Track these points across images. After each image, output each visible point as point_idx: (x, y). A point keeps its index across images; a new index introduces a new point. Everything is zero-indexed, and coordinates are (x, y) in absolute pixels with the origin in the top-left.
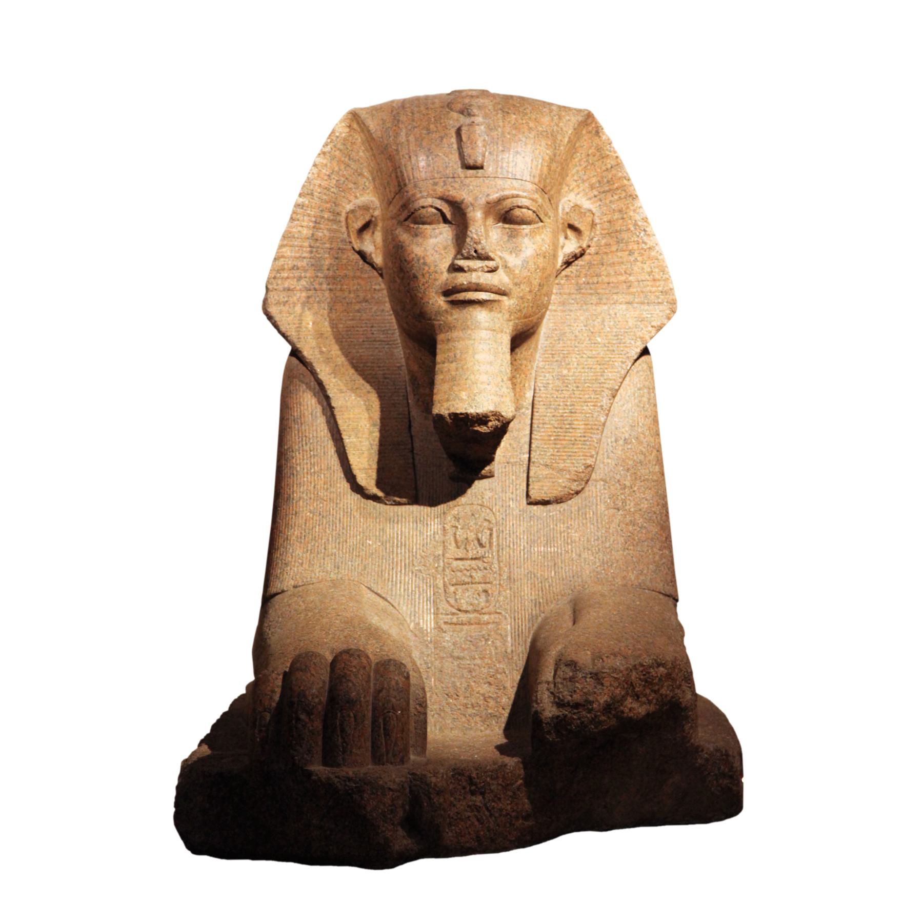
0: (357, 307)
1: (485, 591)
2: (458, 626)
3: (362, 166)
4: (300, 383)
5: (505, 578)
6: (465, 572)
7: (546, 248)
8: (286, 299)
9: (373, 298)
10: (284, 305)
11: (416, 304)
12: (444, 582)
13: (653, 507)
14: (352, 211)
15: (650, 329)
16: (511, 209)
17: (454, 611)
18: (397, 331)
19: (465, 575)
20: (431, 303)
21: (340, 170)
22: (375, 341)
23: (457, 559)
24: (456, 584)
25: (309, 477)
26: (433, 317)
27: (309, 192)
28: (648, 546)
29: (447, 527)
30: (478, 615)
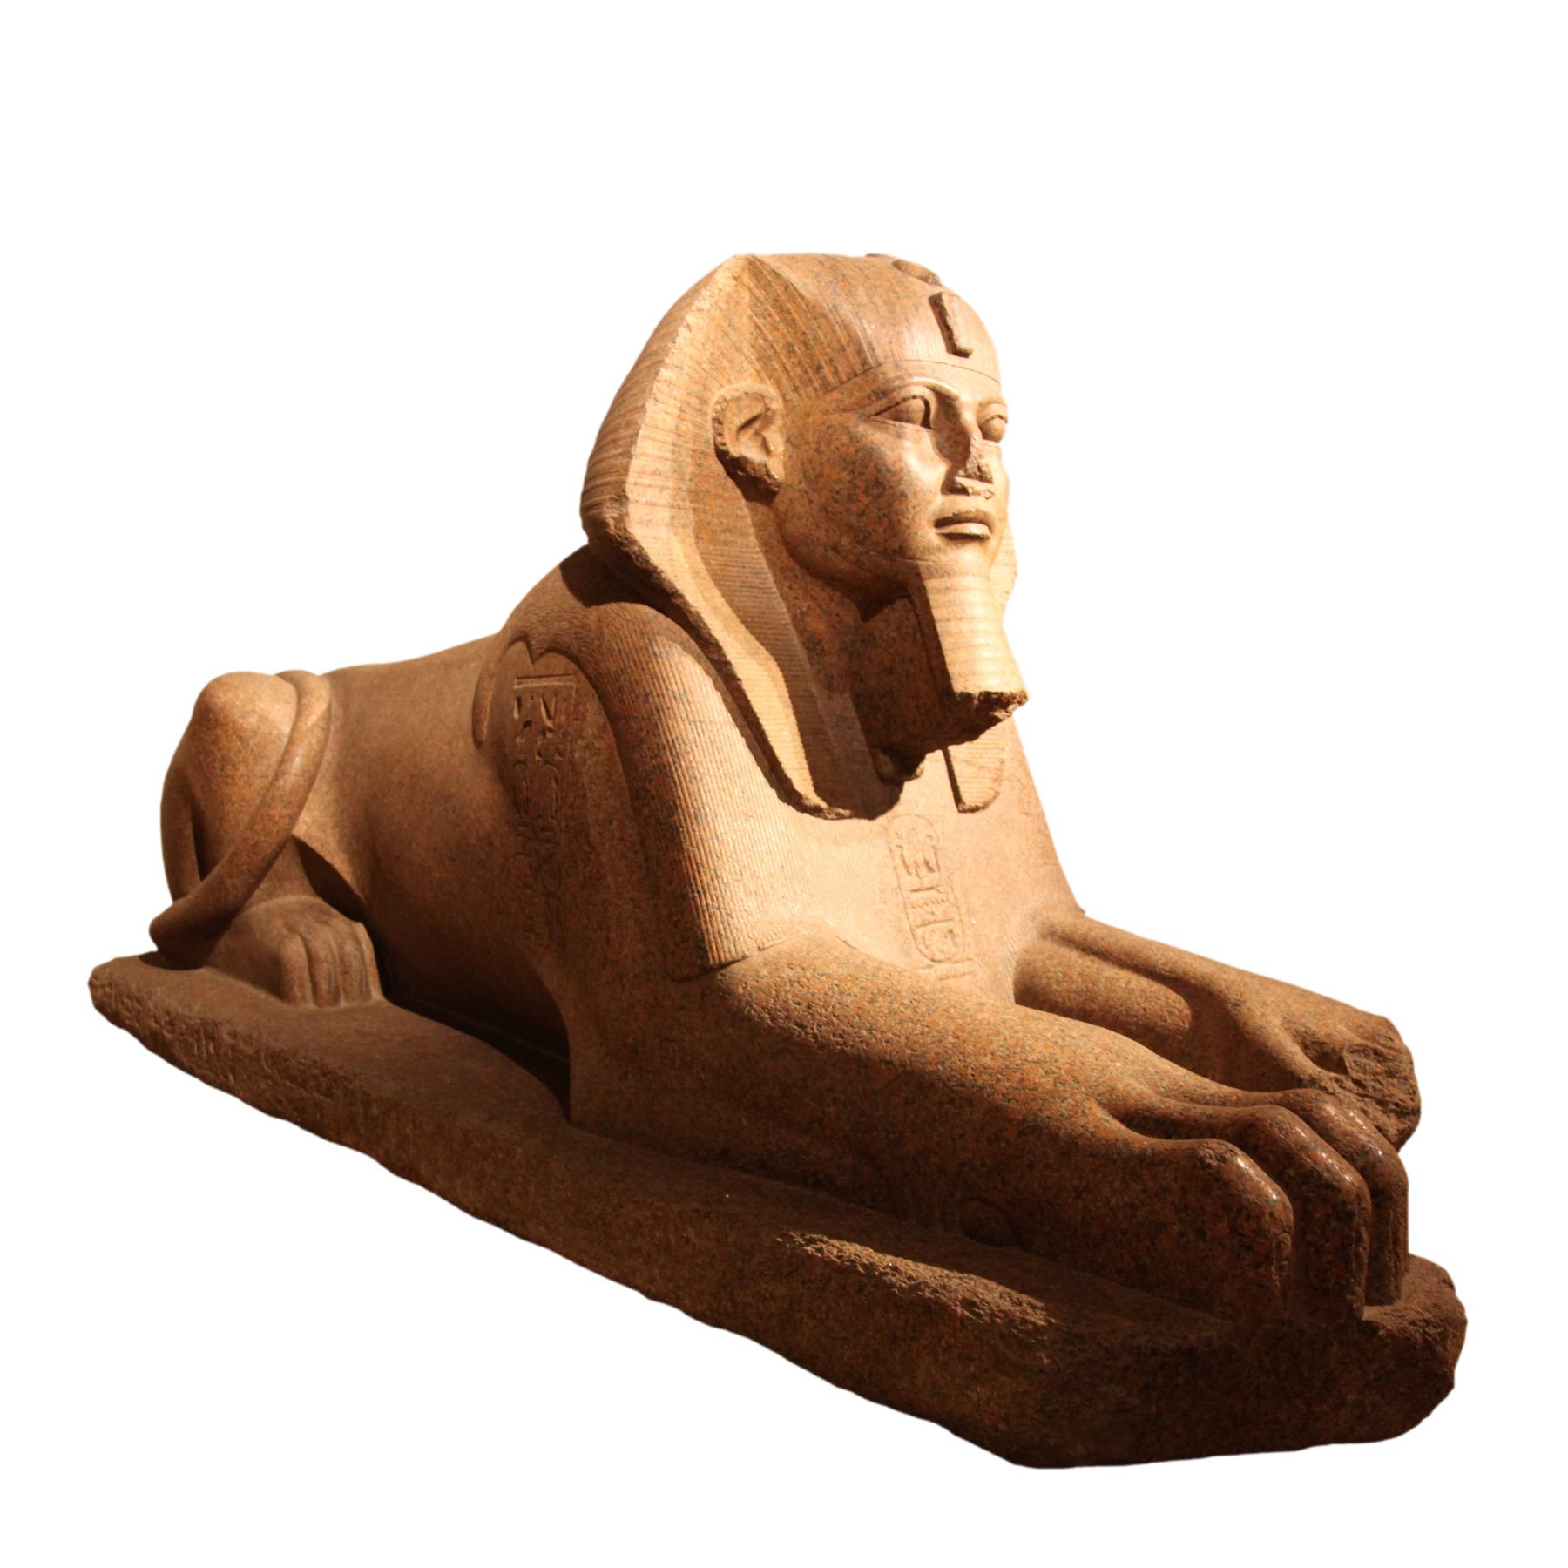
0: (722, 538)
1: (951, 932)
3: (741, 338)
4: (670, 642)
5: (965, 911)
6: (925, 907)
8: (649, 518)
9: (736, 527)
10: (647, 525)
11: (895, 535)
12: (910, 924)
14: (738, 399)
16: (993, 418)
17: (931, 963)
18: (769, 575)
19: (927, 912)
20: (919, 534)
21: (716, 338)
22: (751, 587)
23: (916, 891)
24: (922, 925)
25: (719, 781)
26: (919, 555)
27: (680, 364)
29: (894, 848)
30: (952, 965)
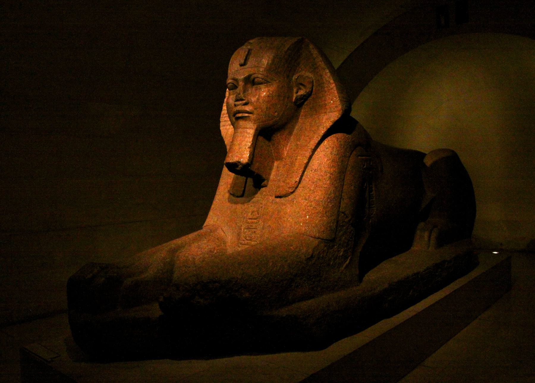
1: (255, 232)
2: (244, 245)
7: (270, 93)
13: (321, 199)
15: (330, 122)
17: (244, 239)
28: (315, 216)
